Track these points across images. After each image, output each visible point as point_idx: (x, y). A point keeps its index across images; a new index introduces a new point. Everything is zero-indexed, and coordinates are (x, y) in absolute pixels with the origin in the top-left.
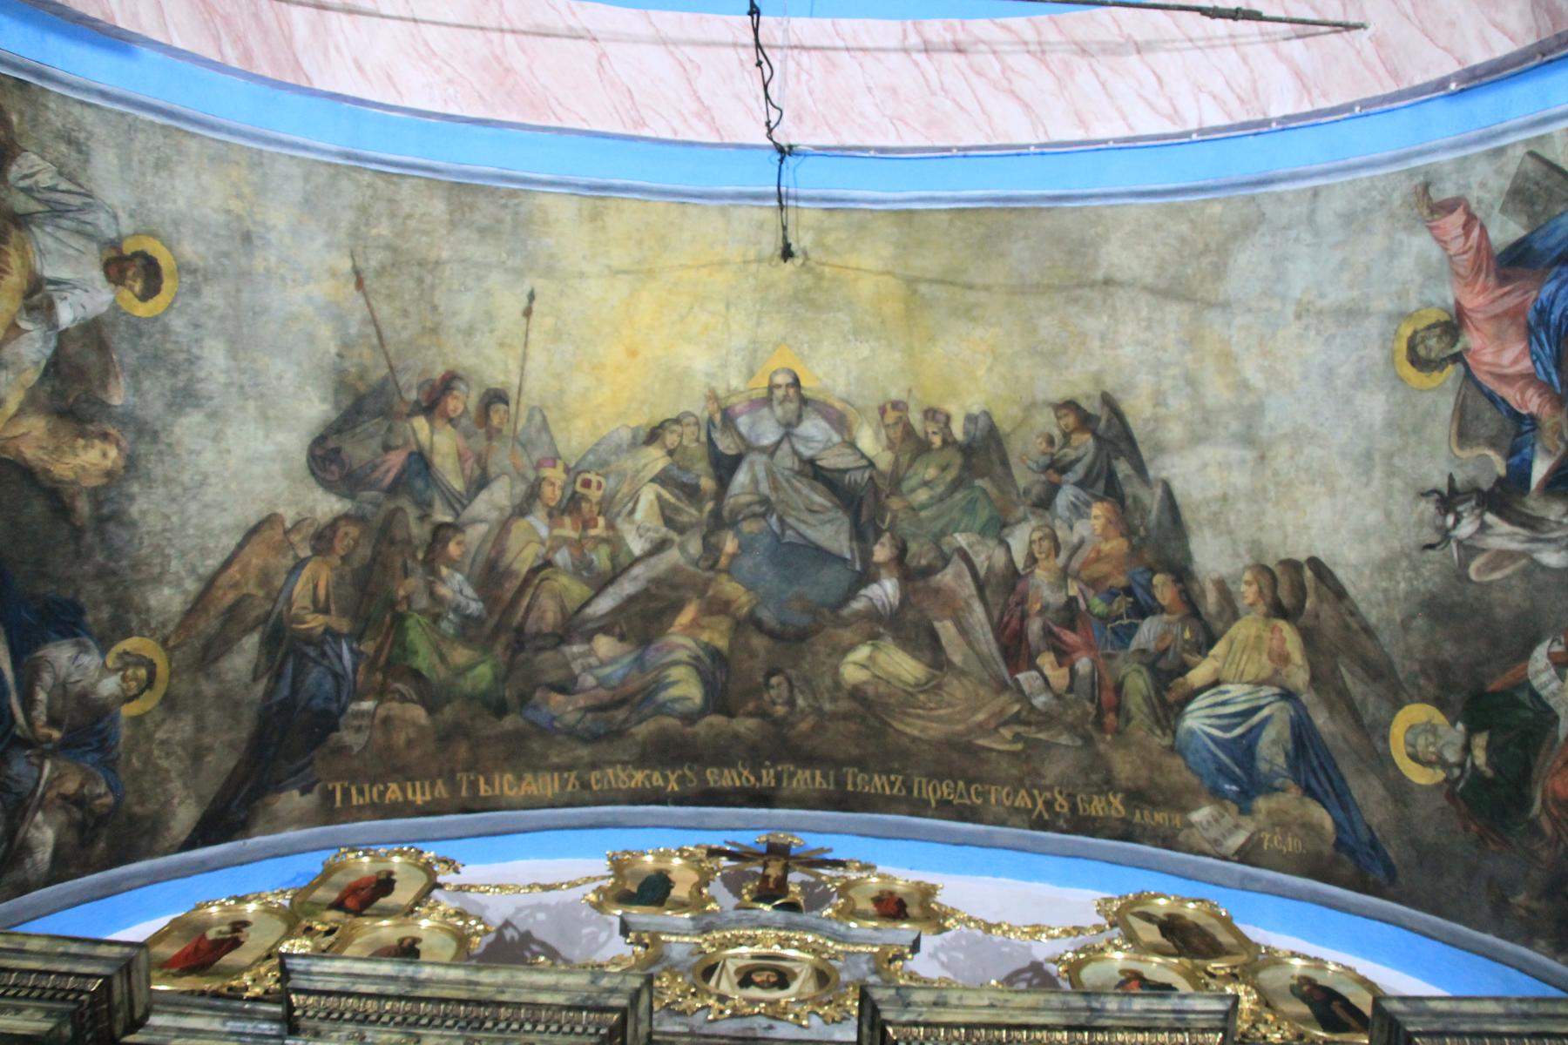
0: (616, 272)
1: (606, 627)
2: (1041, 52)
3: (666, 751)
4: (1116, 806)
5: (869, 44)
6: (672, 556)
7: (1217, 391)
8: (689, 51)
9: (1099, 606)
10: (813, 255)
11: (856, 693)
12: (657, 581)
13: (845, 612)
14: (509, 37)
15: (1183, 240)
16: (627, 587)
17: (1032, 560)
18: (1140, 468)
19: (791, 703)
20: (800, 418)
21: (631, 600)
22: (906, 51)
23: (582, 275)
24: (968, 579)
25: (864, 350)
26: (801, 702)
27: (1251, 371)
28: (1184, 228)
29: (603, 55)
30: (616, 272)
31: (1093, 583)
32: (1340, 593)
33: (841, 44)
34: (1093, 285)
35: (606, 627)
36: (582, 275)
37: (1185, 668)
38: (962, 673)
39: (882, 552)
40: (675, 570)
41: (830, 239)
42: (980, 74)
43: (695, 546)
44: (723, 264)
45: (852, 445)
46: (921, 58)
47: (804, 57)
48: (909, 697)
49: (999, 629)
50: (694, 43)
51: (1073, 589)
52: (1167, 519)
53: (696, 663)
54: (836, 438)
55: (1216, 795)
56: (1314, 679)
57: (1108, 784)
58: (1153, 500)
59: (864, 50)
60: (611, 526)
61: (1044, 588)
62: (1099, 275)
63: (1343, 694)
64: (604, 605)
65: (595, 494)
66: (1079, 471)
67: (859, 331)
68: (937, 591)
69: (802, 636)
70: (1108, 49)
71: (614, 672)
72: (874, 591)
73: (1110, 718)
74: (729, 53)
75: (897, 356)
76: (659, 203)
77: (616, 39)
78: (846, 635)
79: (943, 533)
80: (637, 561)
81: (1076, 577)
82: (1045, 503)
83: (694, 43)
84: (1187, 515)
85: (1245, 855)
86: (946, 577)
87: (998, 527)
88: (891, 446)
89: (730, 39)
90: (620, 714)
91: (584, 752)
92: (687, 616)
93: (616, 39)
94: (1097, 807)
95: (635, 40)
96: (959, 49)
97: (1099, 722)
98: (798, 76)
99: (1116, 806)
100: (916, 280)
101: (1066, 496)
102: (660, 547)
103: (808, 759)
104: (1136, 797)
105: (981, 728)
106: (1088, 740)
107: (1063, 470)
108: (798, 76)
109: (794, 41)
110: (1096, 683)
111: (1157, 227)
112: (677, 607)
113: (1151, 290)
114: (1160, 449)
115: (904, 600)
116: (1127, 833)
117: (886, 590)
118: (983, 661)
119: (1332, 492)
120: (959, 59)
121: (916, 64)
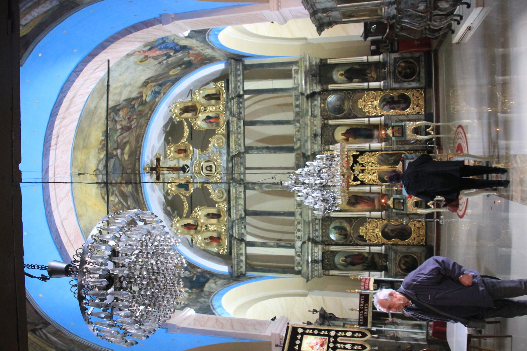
0: (87, 210)
1: (127, 203)
2: (64, 118)
3: (137, 190)
4: (150, 112)
5: (54, 158)
6: (117, 192)
7: (118, 91)
8: (58, 200)
9: (130, 114)
10: (79, 168)
11: (129, 157)
12: (120, 195)
13: (120, 159)
14: (70, 239)
15: (98, 93)
16: (122, 200)
17: (121, 125)
18: (119, 105)
19: (129, 168)
20: (99, 170)
21: (123, 199)
22: (56, 149)
23: (89, 217)
24: (120, 137)
25: (91, 157)
26: (129, 167)
27: (119, 84)
28: (96, 92)
29: (64, 219)
30: (87, 210)
31: (128, 114)
32: (152, 77)
33: (54, 165)
34: (94, 110)
35: (127, 203)
36: (89, 217)
37: (143, 100)
38: (129, 138)
39: (115, 153)
40: (118, 192)
41: (76, 165)
42: (63, 132)
43: (115, 188)
44: (81, 188)
45: (102, 159)
46: (58, 145)
47: (56, 173)
48: (131, 147)
49: (127, 131)
50: (56, 199)
51: (127, 118)
52: (126, 101)
53: (127, 187)
54: (101, 162)
55: (156, 98)
56: (156, 82)
57: (147, 113)
58: (124, 103)
59: (55, 159)
60: (116, 204)
61: (124, 123)
62: (94, 109)
63: (161, 79)
64: (125, 204)
65: (114, 208)
66: (115, 115)
67: (88, 158)
68: (120, 142)
69: (123, 167)
70: (70, 104)
71: (132, 201)
72: (119, 154)
73: (141, 113)
74: (57, 190)
75: (92, 150)
76: (75, 203)
77: (60, 217)
78: (123, 159)
79: (114, 141)
80: (119, 199)
81: (126, 117)
82: (116, 122)
83: (56, 199)
84: (128, 98)
85: (164, 94)
86: (119, 140)
87: (116, 130)
88: (103, 151)
89: (54, 191)
90: (135, 199)
91: (140, 204)
92: (122, 188)
93: (60, 217)
94: (149, 116)
95: (59, 212)
96: (58, 137)
97: (141, 114)
98: (60, 174)
99: (150, 112)
100: (83, 146)
101: (117, 118)
102: (116, 195)
103: (135, 164)
104: (150, 110)
105: (135, 134)
106: (142, 117)
107: (114, 118)
108: (60, 174)
109: (53, 176)
110: (138, 115)
111: (93, 97)
112: (122, 191)
113: (100, 99)
114: (119, 101)
115: (121, 148)
116: (153, 111)
117: (119, 151)
118: (129, 134)
119: (142, 75)
120: (60, 136)
121: (59, 146)
